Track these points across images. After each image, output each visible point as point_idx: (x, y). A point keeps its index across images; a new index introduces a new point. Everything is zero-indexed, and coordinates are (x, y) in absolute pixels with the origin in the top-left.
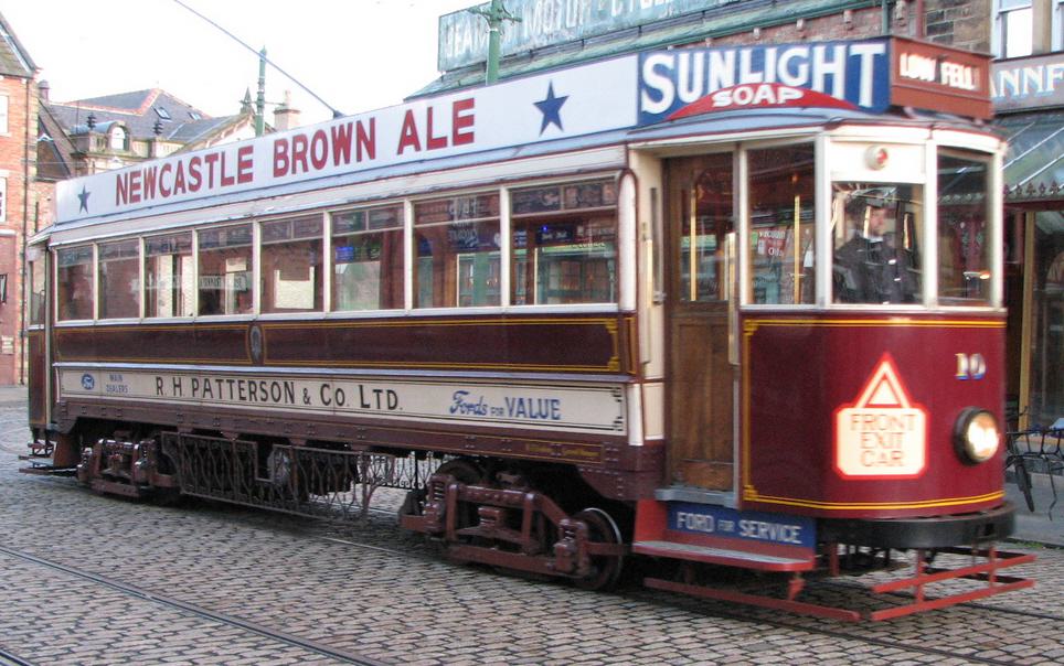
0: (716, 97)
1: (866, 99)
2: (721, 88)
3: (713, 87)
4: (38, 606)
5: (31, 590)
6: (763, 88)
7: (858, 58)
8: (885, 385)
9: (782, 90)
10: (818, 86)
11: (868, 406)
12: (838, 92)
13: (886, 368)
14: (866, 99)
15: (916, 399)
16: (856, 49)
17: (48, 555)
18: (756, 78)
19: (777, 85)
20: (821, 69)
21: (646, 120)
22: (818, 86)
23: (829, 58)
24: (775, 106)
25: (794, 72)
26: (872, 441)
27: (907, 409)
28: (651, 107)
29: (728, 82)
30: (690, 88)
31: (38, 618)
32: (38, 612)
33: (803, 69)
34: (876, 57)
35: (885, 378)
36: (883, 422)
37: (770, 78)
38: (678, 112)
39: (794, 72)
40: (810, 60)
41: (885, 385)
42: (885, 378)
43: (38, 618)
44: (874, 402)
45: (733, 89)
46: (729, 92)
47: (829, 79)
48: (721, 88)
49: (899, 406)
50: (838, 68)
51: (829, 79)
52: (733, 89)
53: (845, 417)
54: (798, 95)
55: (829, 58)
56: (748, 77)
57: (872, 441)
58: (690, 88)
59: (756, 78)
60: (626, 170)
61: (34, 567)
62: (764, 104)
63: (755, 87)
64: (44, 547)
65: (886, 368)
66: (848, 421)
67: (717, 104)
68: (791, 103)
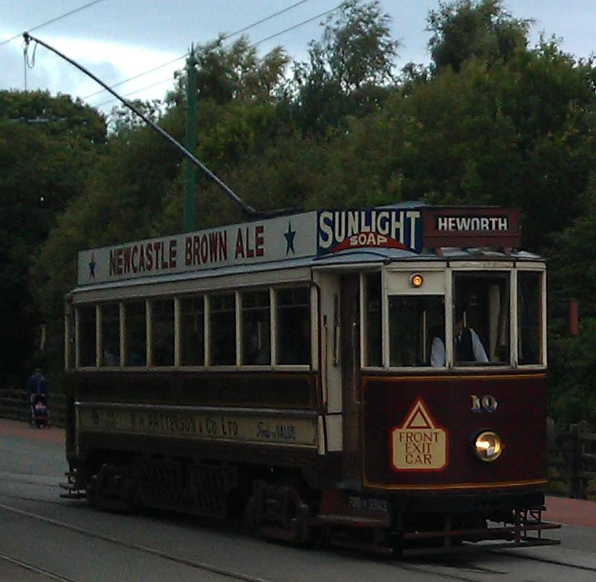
0: (351, 239)
2: (353, 235)
3: (350, 234)
6: (372, 235)
7: (410, 219)
8: (419, 416)
9: (379, 236)
10: (393, 236)
11: (409, 427)
12: (402, 241)
13: (419, 405)
14: (413, 246)
15: (438, 425)
16: (409, 214)
18: (367, 229)
20: (395, 225)
21: (322, 252)
22: (393, 236)
23: (398, 219)
24: (377, 246)
25: (384, 228)
26: (412, 448)
28: (326, 245)
29: (356, 232)
30: (340, 234)
33: (387, 223)
34: (416, 219)
35: (419, 410)
36: (418, 437)
37: (374, 230)
38: (336, 247)
39: (384, 228)
40: (390, 220)
41: (419, 416)
42: (419, 410)
44: (412, 425)
45: (358, 235)
46: (356, 237)
47: (398, 230)
48: (353, 235)
49: (429, 427)
50: (401, 225)
51: (398, 230)
52: (358, 235)
53: (396, 434)
54: (385, 240)
55: (398, 219)
56: (365, 229)
57: (412, 448)
58: (340, 234)
59: (367, 229)
60: (312, 283)
62: (371, 245)
63: (367, 234)
65: (419, 405)
67: (351, 244)
68: (382, 246)
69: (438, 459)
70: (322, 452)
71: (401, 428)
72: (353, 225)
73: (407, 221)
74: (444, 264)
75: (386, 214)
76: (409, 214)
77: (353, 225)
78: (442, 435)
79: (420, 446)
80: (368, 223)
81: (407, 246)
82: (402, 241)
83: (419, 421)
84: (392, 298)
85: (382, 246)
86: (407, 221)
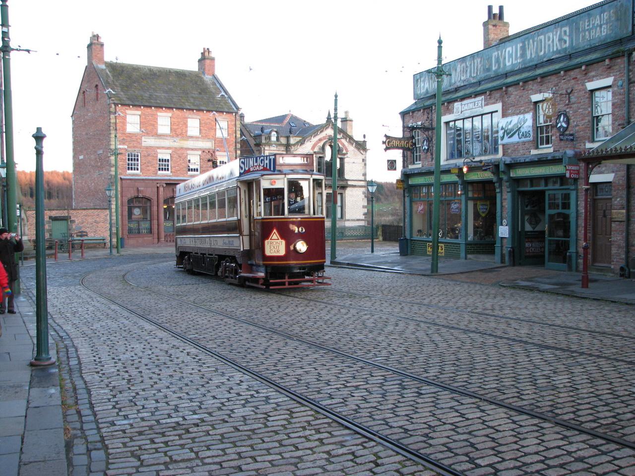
1: (272, 169)
4: (248, 343)
5: (245, 336)
8: (275, 235)
12: (268, 168)
13: (275, 231)
14: (272, 169)
15: (282, 238)
16: (271, 157)
17: (251, 320)
19: (259, 166)
20: (266, 162)
25: (262, 163)
27: (280, 240)
31: (249, 348)
32: (248, 345)
39: (262, 163)
41: (275, 235)
43: (249, 348)
47: (267, 164)
50: (268, 162)
51: (267, 164)
53: (266, 242)
56: (255, 164)
59: (255, 164)
61: (244, 325)
62: (258, 170)
64: (250, 317)
65: (275, 231)
66: (267, 243)
68: (261, 170)
69: (282, 252)
70: (242, 250)
71: (268, 239)
72: (251, 163)
73: (270, 160)
74: (284, 176)
75: (262, 158)
76: (271, 157)
77: (251, 163)
78: (283, 242)
79: (275, 247)
80: (256, 162)
81: (270, 170)
82: (268, 168)
83: (275, 237)
84: (265, 190)
85: (261, 170)
86: (270, 160)
